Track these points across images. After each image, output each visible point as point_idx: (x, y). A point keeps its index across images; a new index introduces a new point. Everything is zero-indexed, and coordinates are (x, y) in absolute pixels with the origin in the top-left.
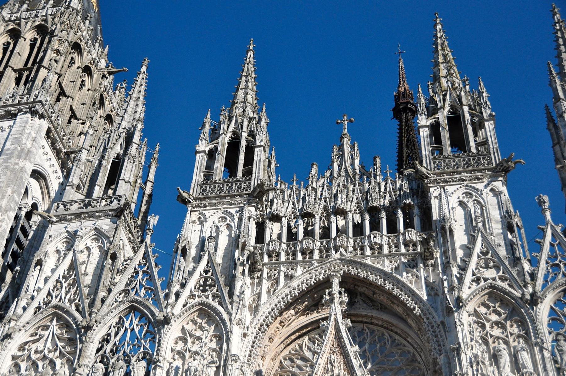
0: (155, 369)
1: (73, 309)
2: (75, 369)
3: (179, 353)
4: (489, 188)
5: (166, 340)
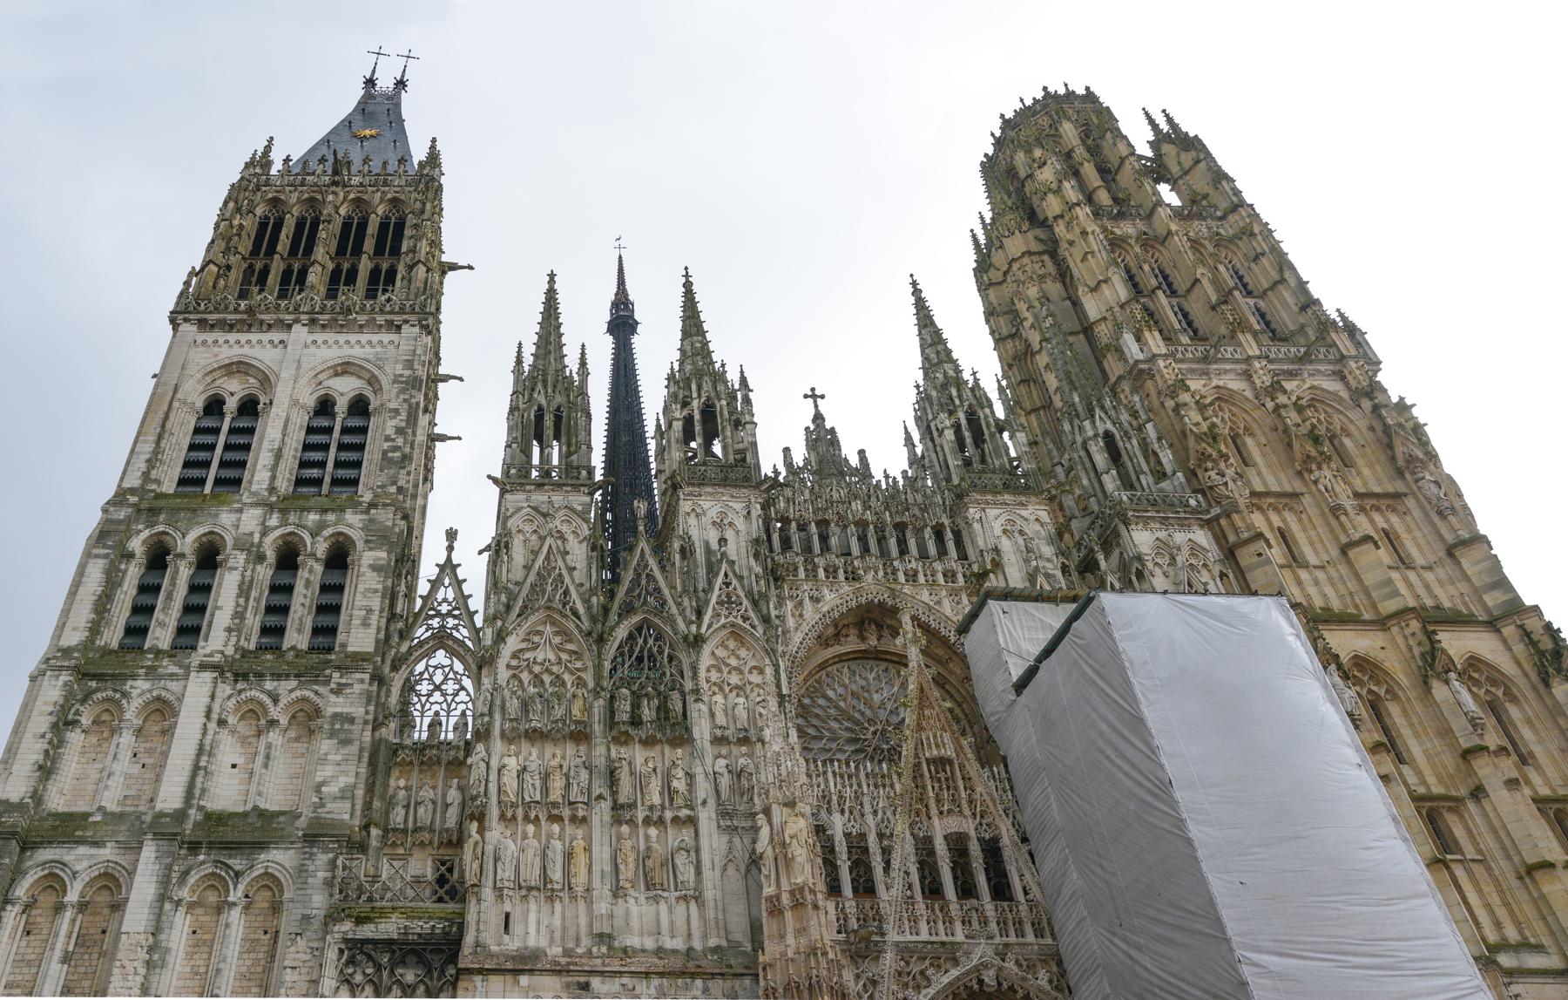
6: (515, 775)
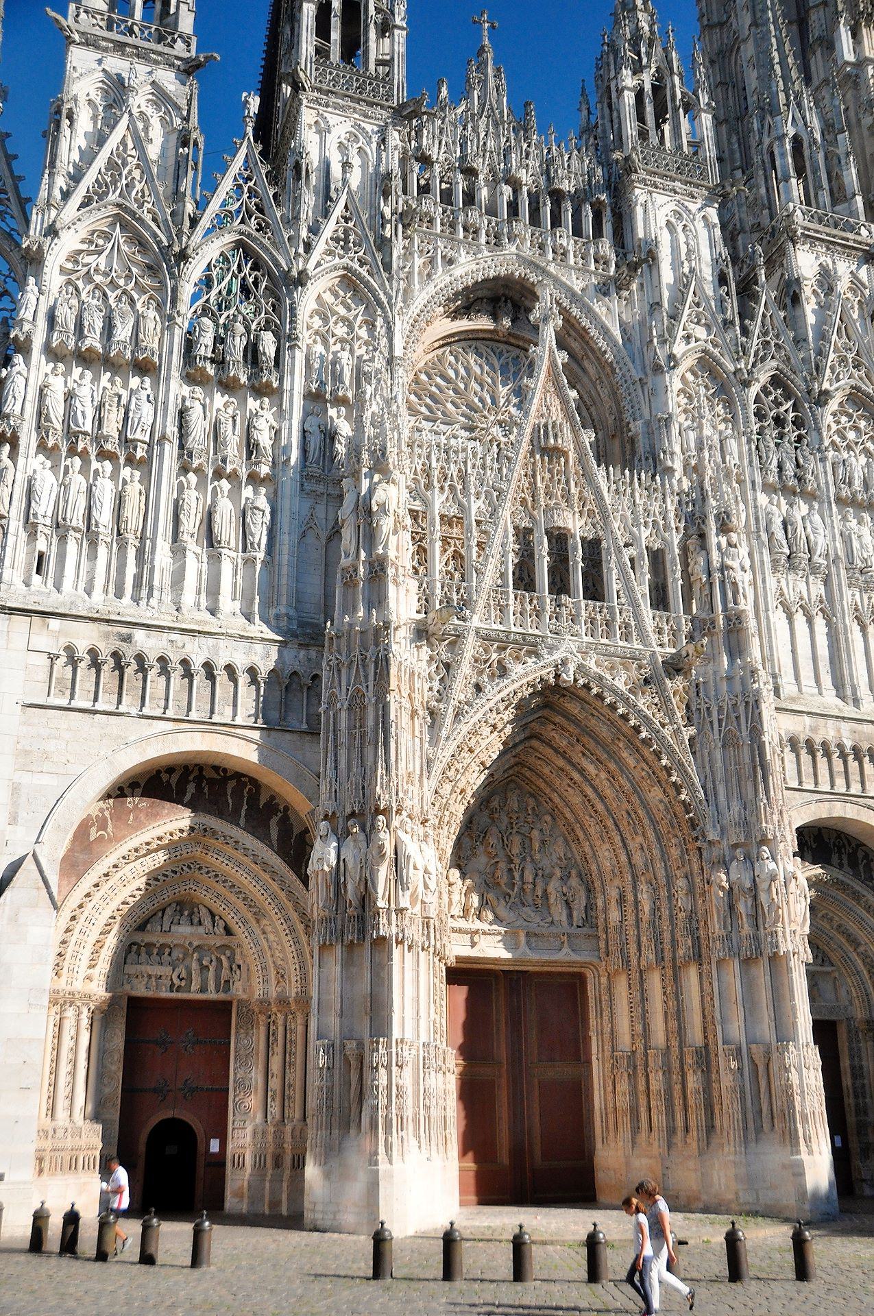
0: (292, 348)
1: (148, 218)
2: (171, 318)
3: (317, 333)
4: (702, 214)
5: (302, 308)
6: (61, 398)
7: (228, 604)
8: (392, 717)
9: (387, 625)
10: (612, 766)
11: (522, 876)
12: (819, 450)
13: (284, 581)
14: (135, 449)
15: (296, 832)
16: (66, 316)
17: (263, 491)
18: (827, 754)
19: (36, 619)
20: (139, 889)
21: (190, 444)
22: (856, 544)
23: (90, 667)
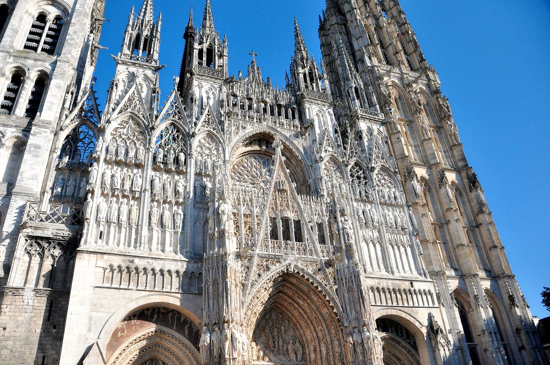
1: (141, 116)
2: (148, 149)
3: (199, 153)
4: (328, 111)
7: (169, 248)
8: (229, 287)
9: (226, 254)
10: (309, 301)
11: (278, 344)
12: (373, 187)
13: (188, 239)
14: (135, 194)
15: (195, 331)
16: (112, 149)
17: (181, 207)
18: (384, 292)
19: (99, 255)
20: (136, 355)
21: (154, 192)
22: (388, 218)
23: (118, 272)
